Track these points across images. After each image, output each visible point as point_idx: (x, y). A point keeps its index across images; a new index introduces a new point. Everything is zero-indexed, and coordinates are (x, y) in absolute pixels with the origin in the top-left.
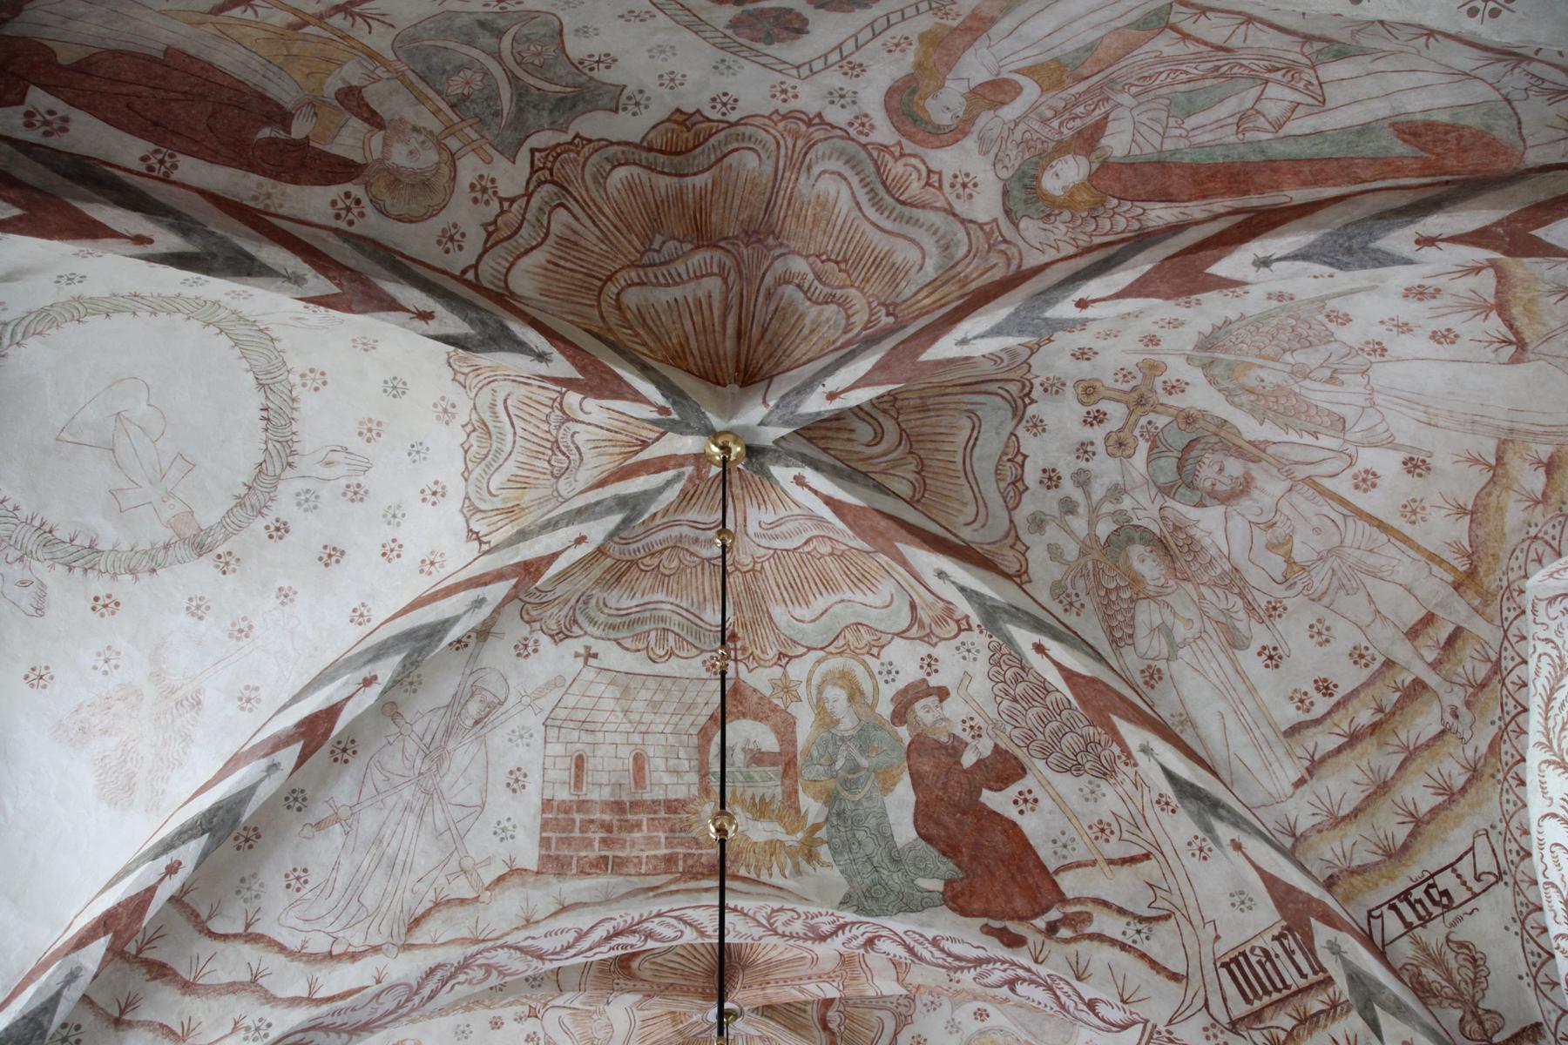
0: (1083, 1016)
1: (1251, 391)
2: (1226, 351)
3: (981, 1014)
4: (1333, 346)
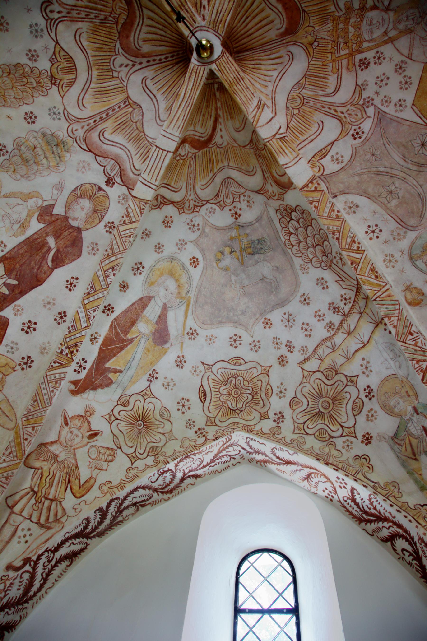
3: (194, 262)
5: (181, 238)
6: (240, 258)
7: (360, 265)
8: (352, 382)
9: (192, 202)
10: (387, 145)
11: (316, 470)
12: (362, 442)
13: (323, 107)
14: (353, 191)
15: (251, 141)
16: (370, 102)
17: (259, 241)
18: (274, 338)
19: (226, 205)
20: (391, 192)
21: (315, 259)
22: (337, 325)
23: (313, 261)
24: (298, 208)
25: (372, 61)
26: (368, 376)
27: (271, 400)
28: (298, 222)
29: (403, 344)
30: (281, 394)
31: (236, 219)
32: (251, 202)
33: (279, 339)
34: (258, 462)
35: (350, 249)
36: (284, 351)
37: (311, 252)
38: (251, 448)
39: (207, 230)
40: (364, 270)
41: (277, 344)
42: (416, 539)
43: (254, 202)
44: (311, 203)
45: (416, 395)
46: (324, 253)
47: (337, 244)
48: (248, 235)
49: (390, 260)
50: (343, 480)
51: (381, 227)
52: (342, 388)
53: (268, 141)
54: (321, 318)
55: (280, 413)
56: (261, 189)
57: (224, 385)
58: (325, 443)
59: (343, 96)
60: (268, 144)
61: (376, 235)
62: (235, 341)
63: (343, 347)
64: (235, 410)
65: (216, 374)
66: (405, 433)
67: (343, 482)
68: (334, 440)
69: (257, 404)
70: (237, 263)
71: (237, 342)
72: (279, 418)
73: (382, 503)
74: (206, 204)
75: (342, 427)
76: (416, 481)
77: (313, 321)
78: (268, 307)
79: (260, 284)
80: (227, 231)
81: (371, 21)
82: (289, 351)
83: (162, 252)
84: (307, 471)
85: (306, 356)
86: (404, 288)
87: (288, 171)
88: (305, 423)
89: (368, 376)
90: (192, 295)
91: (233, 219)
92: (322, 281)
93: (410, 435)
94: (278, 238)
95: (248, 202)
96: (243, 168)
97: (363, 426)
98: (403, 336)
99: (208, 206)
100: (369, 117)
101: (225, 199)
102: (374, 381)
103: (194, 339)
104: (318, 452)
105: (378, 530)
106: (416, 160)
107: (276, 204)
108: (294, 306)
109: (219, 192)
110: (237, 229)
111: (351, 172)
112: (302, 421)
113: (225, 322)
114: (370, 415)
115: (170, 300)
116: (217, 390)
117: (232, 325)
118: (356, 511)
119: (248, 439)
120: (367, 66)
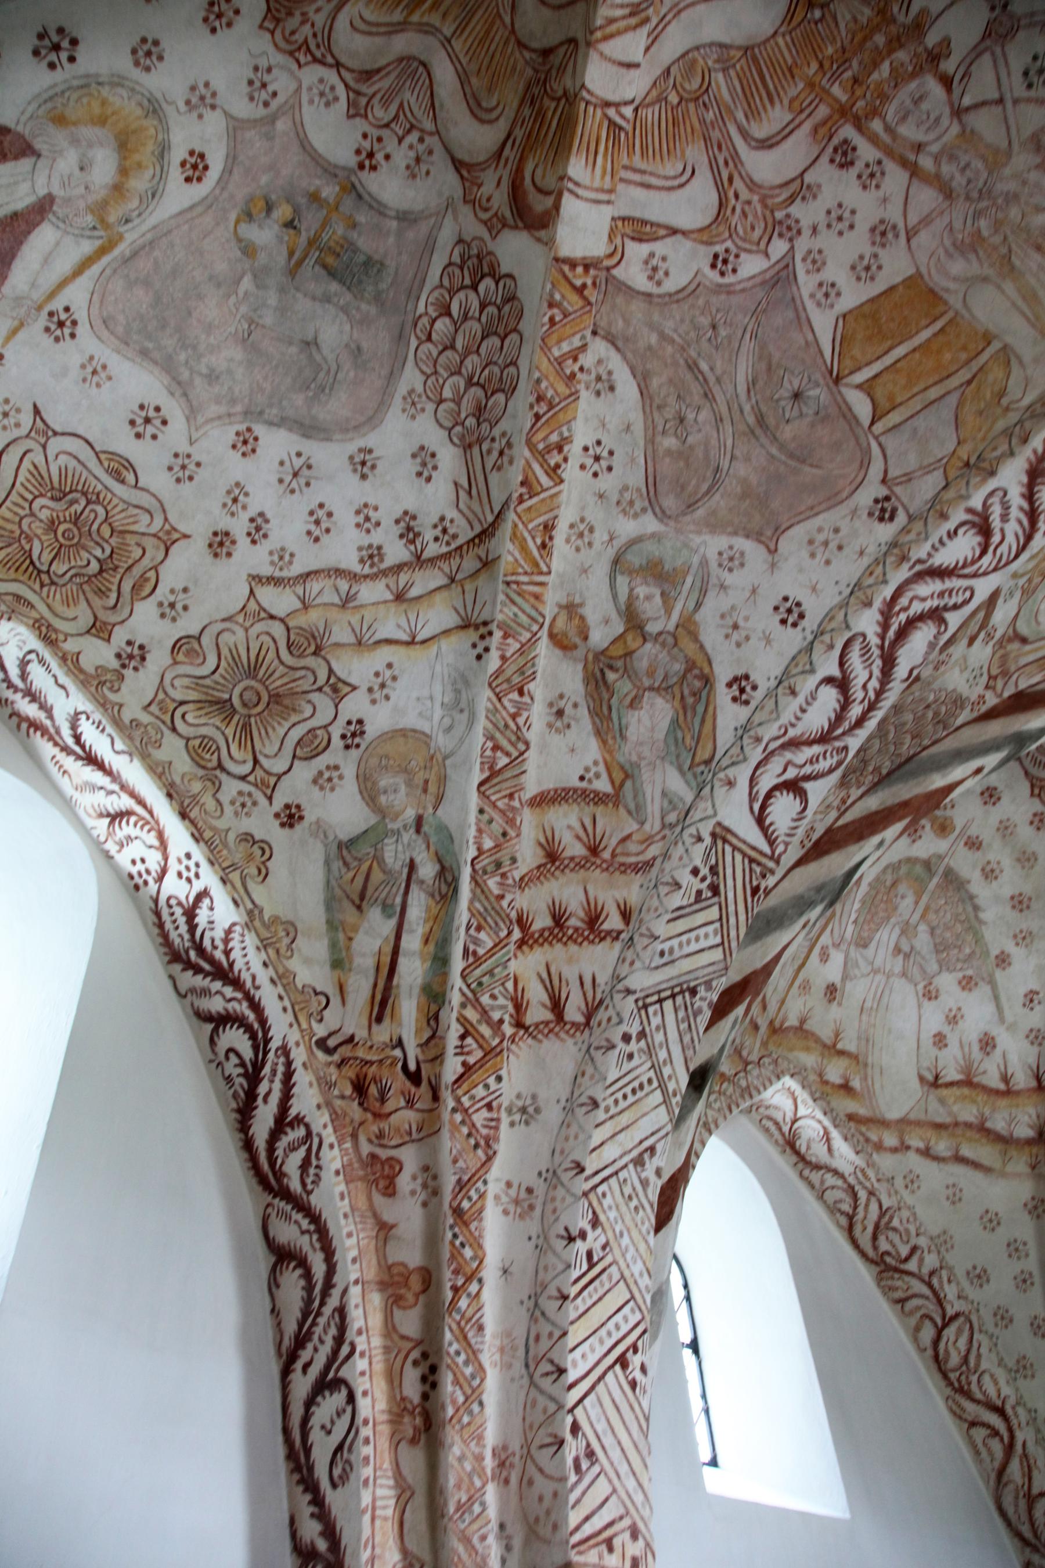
0: (776, 765)
1: (894, 884)
2: (938, 886)
3: (196, 167)
4: (935, 967)
5: (214, 84)
6: (297, 255)
7: (535, 500)
8: (335, 690)
9: (307, 29)
10: (748, 336)
11: (151, 813)
12: (277, 815)
13: (720, 147)
14: (629, 355)
15: (546, 53)
16: (790, 230)
17: (369, 263)
18: (237, 484)
19: (366, 116)
20: (682, 420)
21: (452, 405)
22: (389, 561)
23: (443, 407)
24: (509, 281)
25: (859, 165)
26: (374, 702)
27: (139, 606)
28: (483, 306)
29: (494, 699)
30: (170, 610)
31: (361, 166)
32: (424, 168)
33: (246, 494)
34: (14, 714)
35: (541, 456)
36: (239, 526)
37: (455, 388)
38: (24, 676)
39: (281, 125)
40: (533, 514)
41: (235, 500)
42: (274, 1045)
43: (428, 173)
44: (551, 305)
45: (439, 800)
46: (479, 412)
47: (529, 425)
48: (354, 226)
49: (583, 531)
50: (197, 865)
51: (616, 461)
52: (306, 688)
53: (587, 103)
54: (367, 525)
55: (141, 647)
56: (470, 167)
57: (52, 498)
58: (201, 772)
59: (767, 167)
60: (583, 105)
61: (596, 467)
62: (147, 420)
63: (368, 615)
64: (39, 572)
65: (50, 458)
66: (372, 851)
67: (193, 869)
68: (223, 777)
69: (102, 593)
70: (281, 259)
71: (149, 428)
72: (131, 657)
73: (251, 951)
74: (331, 66)
75: (256, 761)
76: (334, 945)
77: (345, 518)
78: (275, 411)
79: (293, 350)
80: (319, 171)
81: (921, 98)
82: (249, 534)
83: (148, 69)
84: (125, 802)
85: (277, 574)
86: (564, 602)
87: (567, 200)
88: (182, 703)
89: (374, 702)
90: (131, 237)
91: (352, 161)
92: (428, 459)
93: (378, 858)
94: (413, 294)
95: (418, 160)
96: (474, 81)
97: (297, 786)
98: (505, 686)
99: (331, 76)
100: (767, 255)
101: (375, 101)
102: (379, 721)
103: (57, 339)
104: (178, 780)
105: (205, 992)
106: (764, 409)
107: (472, 228)
108: (330, 456)
109: (378, 71)
110: (343, 189)
111: (656, 317)
112: (178, 696)
113: (156, 363)
114: (326, 775)
115: (69, 199)
116: (30, 497)
117: (166, 380)
118: (180, 936)
119: (33, 656)
120: (844, 166)
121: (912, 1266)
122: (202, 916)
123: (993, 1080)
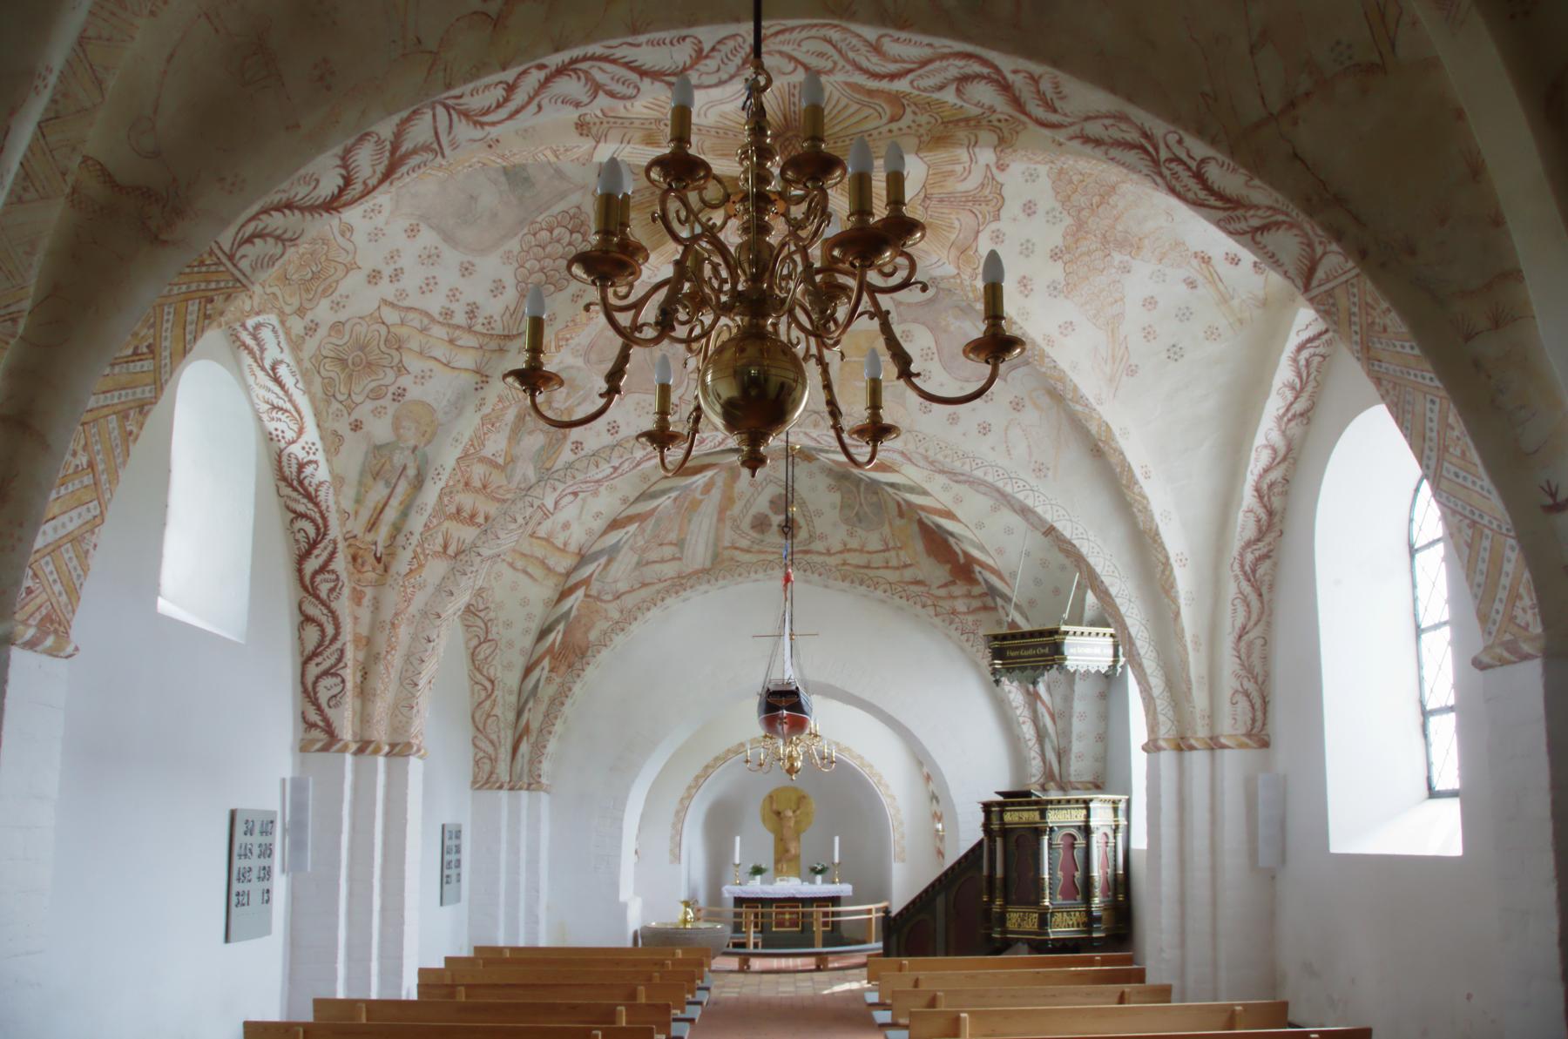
28: (570, 244)
35: (558, 339)
45: (429, 442)
76: (358, 493)
93: (391, 459)
97: (364, 411)
102: (414, 392)
105: (297, 501)
121: (482, 614)
122: (308, 470)
123: (559, 543)
